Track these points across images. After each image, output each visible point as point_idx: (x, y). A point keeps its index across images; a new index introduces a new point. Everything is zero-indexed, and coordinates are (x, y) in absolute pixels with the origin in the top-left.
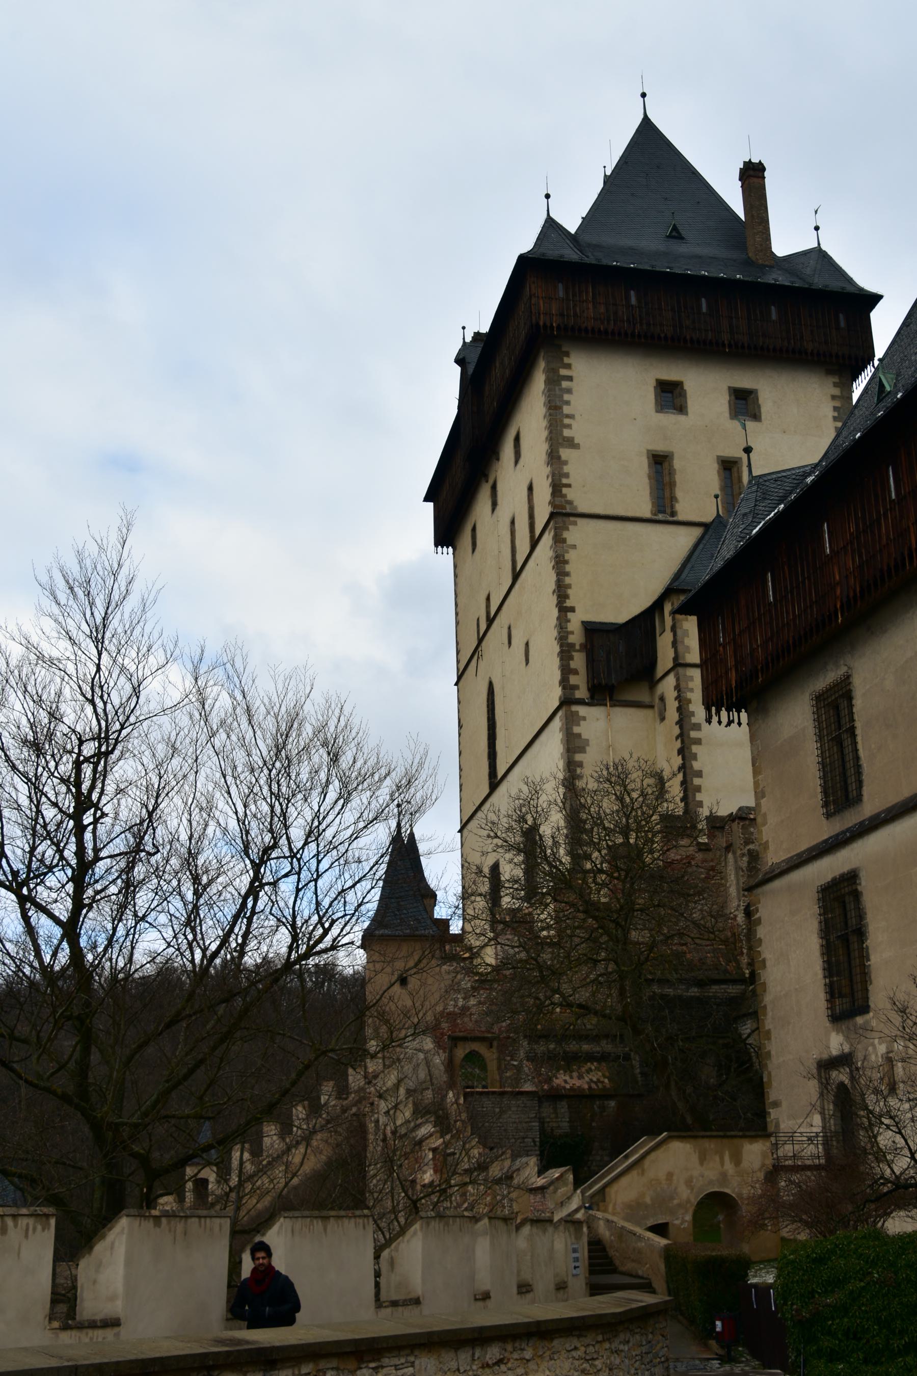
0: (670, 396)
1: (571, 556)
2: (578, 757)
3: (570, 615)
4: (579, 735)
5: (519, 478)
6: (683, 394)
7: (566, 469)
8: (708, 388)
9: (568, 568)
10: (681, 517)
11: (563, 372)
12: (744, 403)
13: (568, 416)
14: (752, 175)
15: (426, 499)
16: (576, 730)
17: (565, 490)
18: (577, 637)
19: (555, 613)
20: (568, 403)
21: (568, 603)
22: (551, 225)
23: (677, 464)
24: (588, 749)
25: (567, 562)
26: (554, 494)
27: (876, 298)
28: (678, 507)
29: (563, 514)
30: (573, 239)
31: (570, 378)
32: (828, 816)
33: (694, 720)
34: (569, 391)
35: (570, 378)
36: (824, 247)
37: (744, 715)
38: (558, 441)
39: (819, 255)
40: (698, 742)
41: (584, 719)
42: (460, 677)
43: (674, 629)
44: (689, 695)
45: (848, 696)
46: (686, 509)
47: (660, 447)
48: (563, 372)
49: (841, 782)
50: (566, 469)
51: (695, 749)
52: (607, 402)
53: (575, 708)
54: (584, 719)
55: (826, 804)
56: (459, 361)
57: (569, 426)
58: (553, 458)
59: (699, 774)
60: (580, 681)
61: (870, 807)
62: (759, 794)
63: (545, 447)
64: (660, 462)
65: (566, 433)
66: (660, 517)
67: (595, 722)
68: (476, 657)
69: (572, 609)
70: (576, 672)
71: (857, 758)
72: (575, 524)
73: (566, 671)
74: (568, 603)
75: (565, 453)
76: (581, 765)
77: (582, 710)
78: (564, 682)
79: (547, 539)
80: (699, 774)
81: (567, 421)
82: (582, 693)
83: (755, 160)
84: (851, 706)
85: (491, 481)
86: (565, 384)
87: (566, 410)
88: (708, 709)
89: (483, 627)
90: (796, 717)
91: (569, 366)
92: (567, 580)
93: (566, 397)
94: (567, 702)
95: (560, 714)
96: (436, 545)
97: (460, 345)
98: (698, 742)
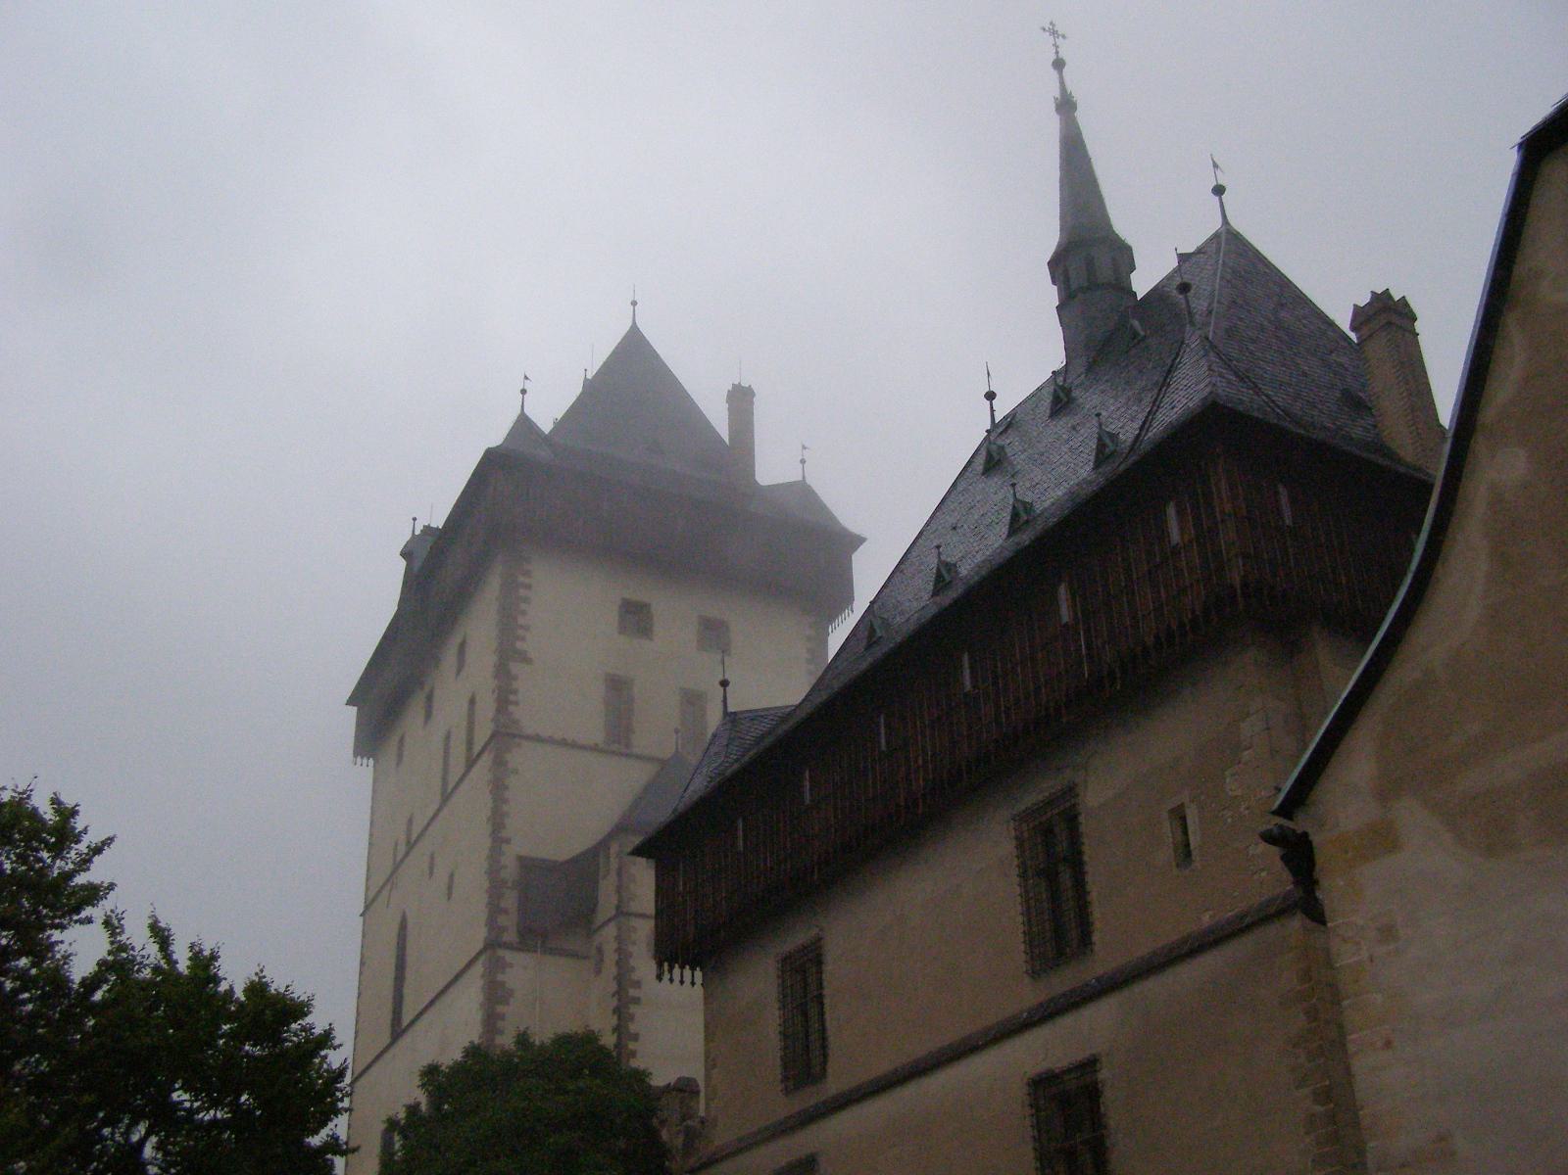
0: (636, 618)
2: (500, 1009)
3: (505, 847)
4: (503, 984)
5: (460, 687)
7: (515, 685)
8: (677, 614)
10: (636, 750)
11: (521, 579)
12: (713, 634)
13: (521, 627)
14: (741, 399)
15: (350, 702)
16: (500, 977)
17: (511, 708)
18: (510, 871)
19: (487, 843)
20: (524, 613)
21: (504, 834)
22: (524, 424)
24: (512, 1000)
25: (507, 788)
26: (498, 711)
29: (506, 735)
30: (547, 440)
31: (529, 587)
32: (787, 1092)
33: (635, 977)
34: (526, 600)
35: (529, 587)
36: (808, 481)
37: (698, 974)
38: (509, 655)
39: (802, 491)
40: (636, 1001)
41: (511, 966)
42: (367, 907)
43: (619, 874)
44: (631, 948)
45: (819, 962)
46: (642, 742)
48: (521, 579)
49: (804, 1054)
50: (515, 685)
51: (633, 1009)
52: (564, 618)
53: (501, 952)
54: (511, 966)
55: (785, 1079)
56: (406, 554)
57: (523, 639)
58: (502, 672)
59: (635, 1037)
60: (509, 921)
61: (836, 1082)
62: (711, 1063)
63: (493, 659)
64: (617, 687)
65: (519, 645)
66: (615, 747)
67: (522, 971)
68: (388, 887)
69: (508, 841)
70: (506, 911)
71: (823, 1029)
72: (519, 745)
73: (495, 910)
74: (504, 834)
75: (516, 668)
76: (502, 1017)
77: (509, 956)
78: (491, 923)
79: (486, 760)
80: (635, 1037)
81: (520, 632)
82: (511, 936)
83: (745, 384)
84: (820, 972)
85: (427, 689)
86: (522, 592)
87: (521, 621)
88: (660, 965)
89: (402, 849)
90: (758, 981)
91: (527, 574)
92: (505, 808)
93: (523, 606)
94: (492, 945)
95: (483, 958)
96: (356, 755)
97: (408, 537)
98: (636, 1001)
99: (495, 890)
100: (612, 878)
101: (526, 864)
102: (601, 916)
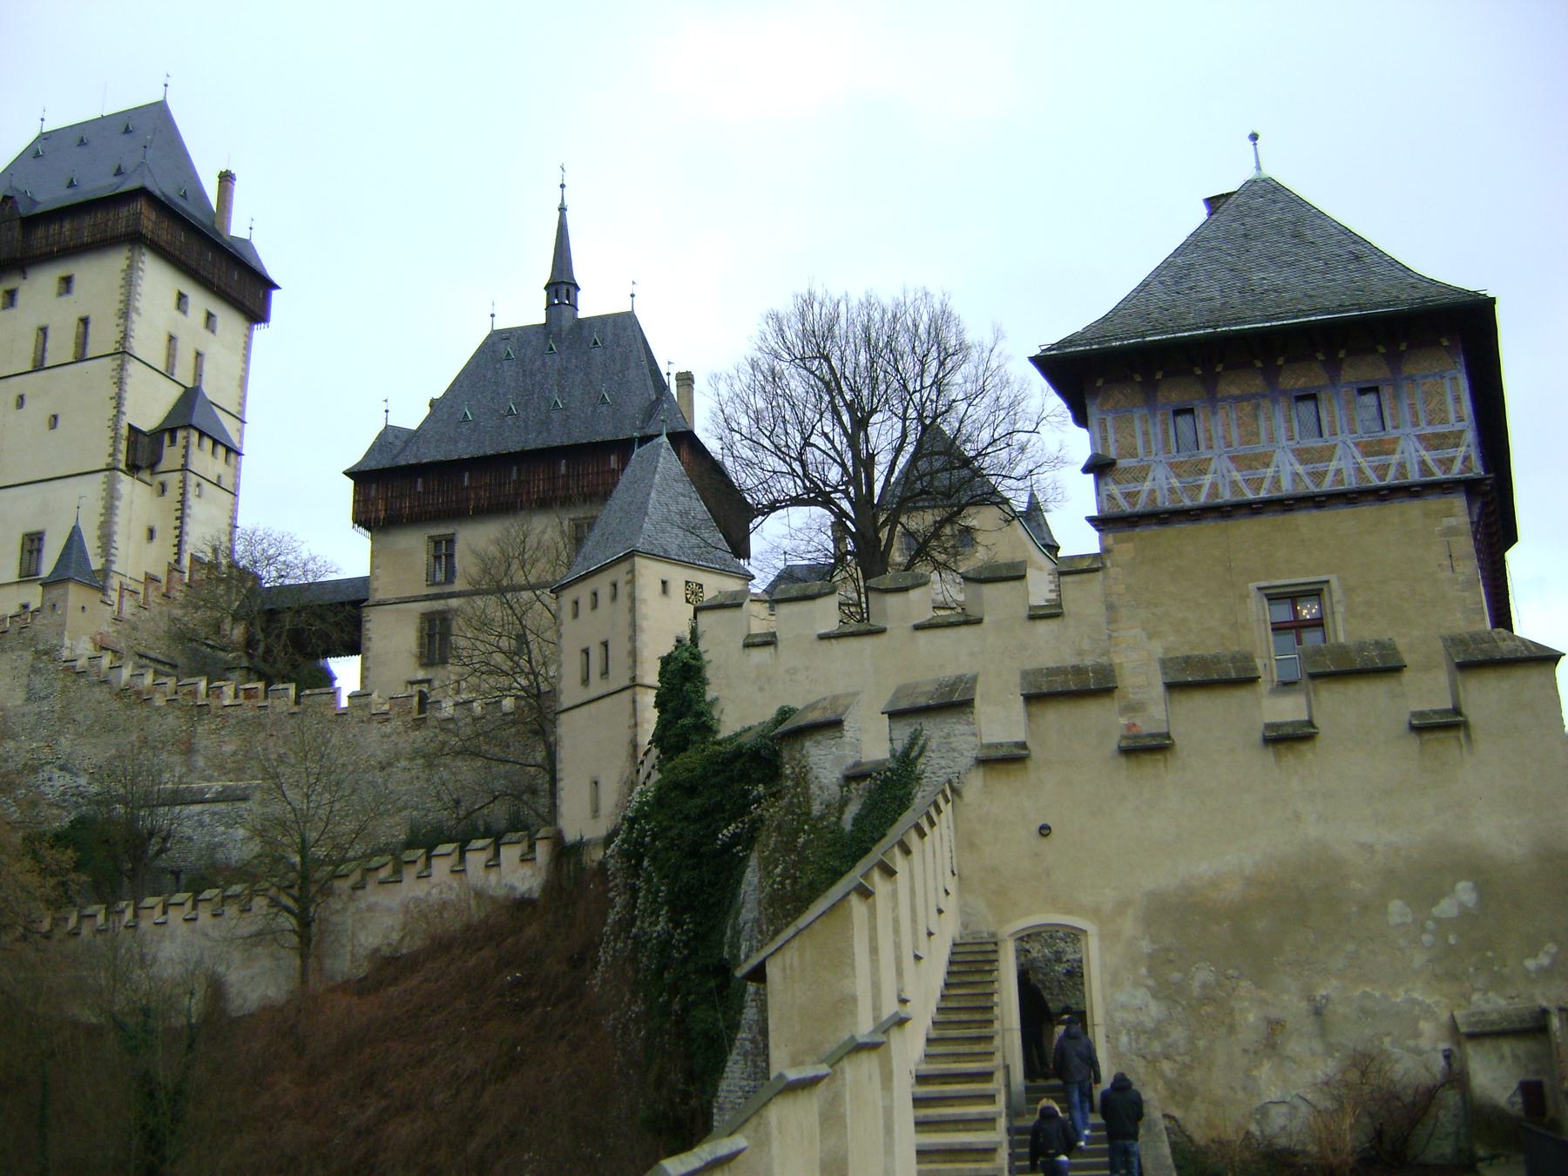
1: (128, 381)
6: (186, 303)
9: (127, 388)
18: (124, 431)
23: (179, 345)
27: (277, 287)
28: (176, 371)
39: (247, 243)
47: (174, 333)
60: (122, 457)
64: (171, 338)
67: (126, 484)
75: (134, 316)
82: (122, 466)
94: (111, 468)
99: (115, 439)
100: (178, 450)
101: (130, 426)
102: (162, 467)
